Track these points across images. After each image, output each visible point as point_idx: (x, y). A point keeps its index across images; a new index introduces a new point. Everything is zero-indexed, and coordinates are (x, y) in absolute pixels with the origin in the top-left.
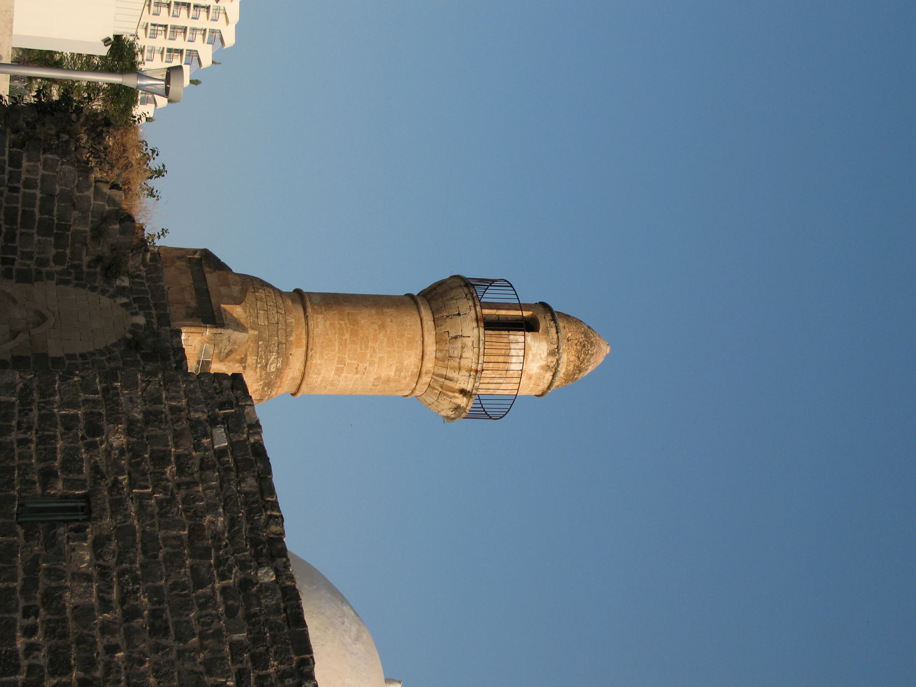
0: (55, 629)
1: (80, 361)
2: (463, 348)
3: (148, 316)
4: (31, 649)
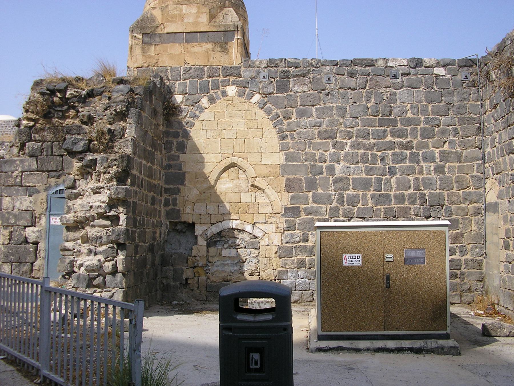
1: (289, 140)
3: (226, 84)
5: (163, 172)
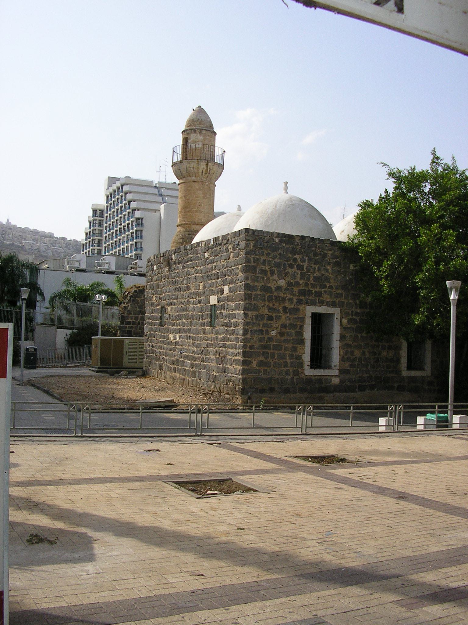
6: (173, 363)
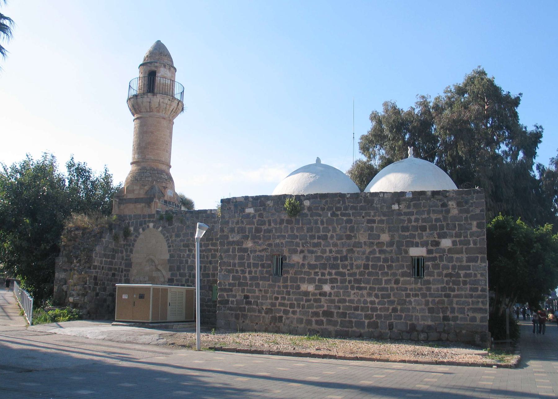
0: (324, 266)
1: (172, 248)
2: (163, 103)
3: (149, 222)
4: (330, 274)
5: (123, 262)
6: (316, 314)
